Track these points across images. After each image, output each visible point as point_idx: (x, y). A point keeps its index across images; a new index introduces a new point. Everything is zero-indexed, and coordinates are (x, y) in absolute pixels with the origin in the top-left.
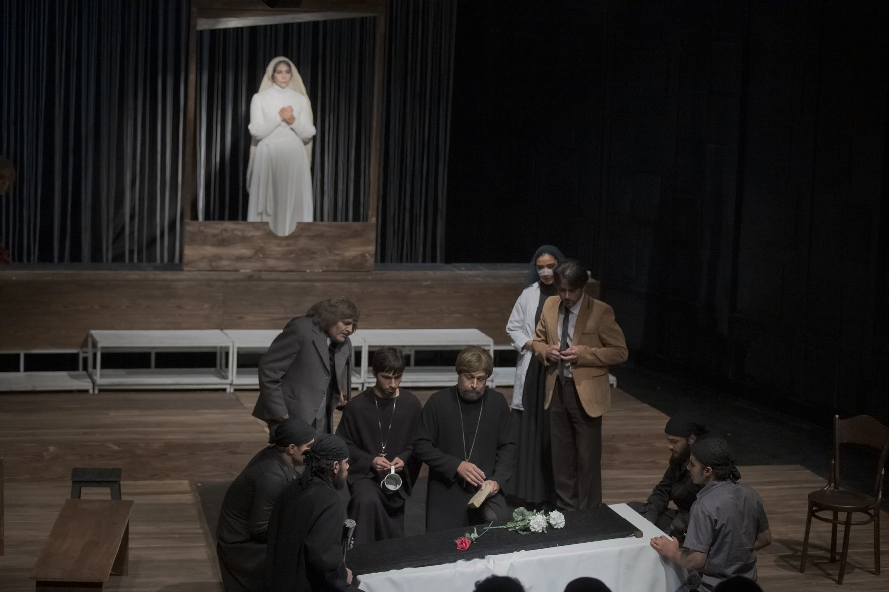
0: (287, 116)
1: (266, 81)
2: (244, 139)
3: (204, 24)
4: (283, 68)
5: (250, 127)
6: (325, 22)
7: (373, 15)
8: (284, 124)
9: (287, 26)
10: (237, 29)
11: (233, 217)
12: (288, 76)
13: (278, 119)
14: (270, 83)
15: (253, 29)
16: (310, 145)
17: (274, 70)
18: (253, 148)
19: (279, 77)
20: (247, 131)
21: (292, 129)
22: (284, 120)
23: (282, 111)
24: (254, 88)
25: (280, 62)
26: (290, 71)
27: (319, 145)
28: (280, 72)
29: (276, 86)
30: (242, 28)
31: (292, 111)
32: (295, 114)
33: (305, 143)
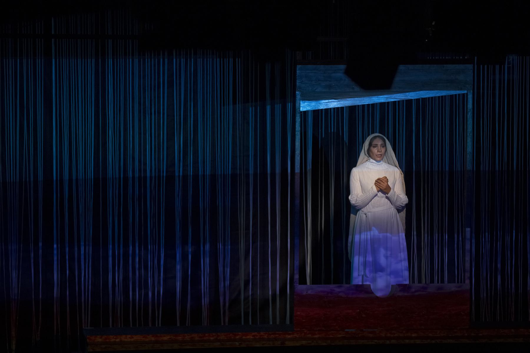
0: (384, 186)
1: (362, 156)
2: (345, 209)
3: (305, 106)
4: (379, 142)
5: (350, 198)
6: (418, 100)
7: (465, 92)
8: (380, 194)
9: (382, 104)
10: (338, 108)
11: (338, 281)
12: (383, 150)
13: (375, 189)
14: (366, 158)
15: (352, 109)
16: (403, 214)
17: (370, 145)
18: (352, 216)
19: (375, 150)
20: (348, 201)
21: (387, 198)
22: (380, 190)
23: (378, 182)
24: (353, 163)
25: (375, 137)
26: (384, 145)
27: (411, 212)
28: (376, 146)
29: (372, 160)
30: (342, 108)
31: (387, 181)
32: (389, 183)
33: (399, 211)
